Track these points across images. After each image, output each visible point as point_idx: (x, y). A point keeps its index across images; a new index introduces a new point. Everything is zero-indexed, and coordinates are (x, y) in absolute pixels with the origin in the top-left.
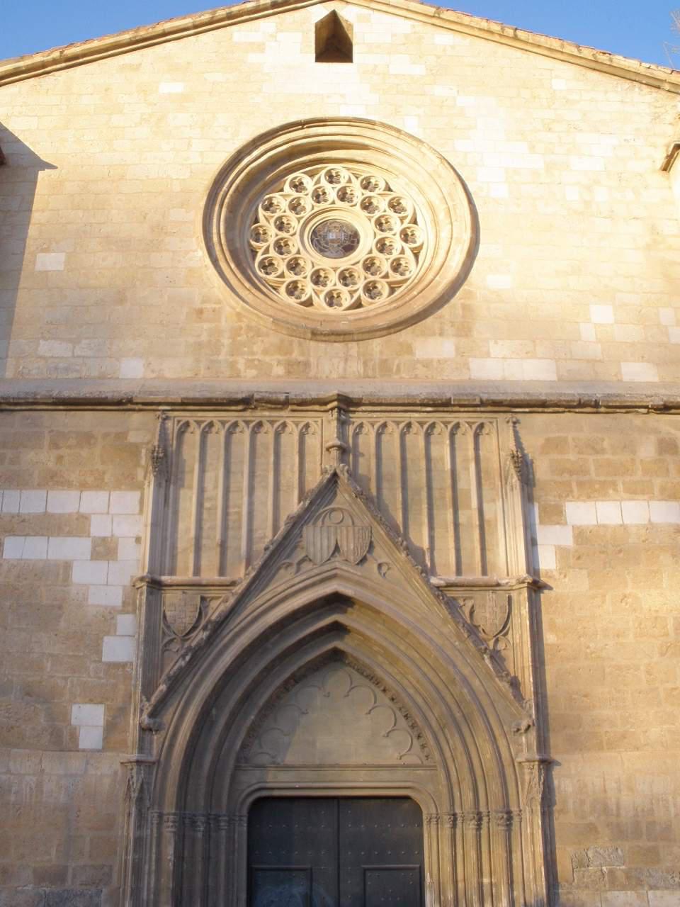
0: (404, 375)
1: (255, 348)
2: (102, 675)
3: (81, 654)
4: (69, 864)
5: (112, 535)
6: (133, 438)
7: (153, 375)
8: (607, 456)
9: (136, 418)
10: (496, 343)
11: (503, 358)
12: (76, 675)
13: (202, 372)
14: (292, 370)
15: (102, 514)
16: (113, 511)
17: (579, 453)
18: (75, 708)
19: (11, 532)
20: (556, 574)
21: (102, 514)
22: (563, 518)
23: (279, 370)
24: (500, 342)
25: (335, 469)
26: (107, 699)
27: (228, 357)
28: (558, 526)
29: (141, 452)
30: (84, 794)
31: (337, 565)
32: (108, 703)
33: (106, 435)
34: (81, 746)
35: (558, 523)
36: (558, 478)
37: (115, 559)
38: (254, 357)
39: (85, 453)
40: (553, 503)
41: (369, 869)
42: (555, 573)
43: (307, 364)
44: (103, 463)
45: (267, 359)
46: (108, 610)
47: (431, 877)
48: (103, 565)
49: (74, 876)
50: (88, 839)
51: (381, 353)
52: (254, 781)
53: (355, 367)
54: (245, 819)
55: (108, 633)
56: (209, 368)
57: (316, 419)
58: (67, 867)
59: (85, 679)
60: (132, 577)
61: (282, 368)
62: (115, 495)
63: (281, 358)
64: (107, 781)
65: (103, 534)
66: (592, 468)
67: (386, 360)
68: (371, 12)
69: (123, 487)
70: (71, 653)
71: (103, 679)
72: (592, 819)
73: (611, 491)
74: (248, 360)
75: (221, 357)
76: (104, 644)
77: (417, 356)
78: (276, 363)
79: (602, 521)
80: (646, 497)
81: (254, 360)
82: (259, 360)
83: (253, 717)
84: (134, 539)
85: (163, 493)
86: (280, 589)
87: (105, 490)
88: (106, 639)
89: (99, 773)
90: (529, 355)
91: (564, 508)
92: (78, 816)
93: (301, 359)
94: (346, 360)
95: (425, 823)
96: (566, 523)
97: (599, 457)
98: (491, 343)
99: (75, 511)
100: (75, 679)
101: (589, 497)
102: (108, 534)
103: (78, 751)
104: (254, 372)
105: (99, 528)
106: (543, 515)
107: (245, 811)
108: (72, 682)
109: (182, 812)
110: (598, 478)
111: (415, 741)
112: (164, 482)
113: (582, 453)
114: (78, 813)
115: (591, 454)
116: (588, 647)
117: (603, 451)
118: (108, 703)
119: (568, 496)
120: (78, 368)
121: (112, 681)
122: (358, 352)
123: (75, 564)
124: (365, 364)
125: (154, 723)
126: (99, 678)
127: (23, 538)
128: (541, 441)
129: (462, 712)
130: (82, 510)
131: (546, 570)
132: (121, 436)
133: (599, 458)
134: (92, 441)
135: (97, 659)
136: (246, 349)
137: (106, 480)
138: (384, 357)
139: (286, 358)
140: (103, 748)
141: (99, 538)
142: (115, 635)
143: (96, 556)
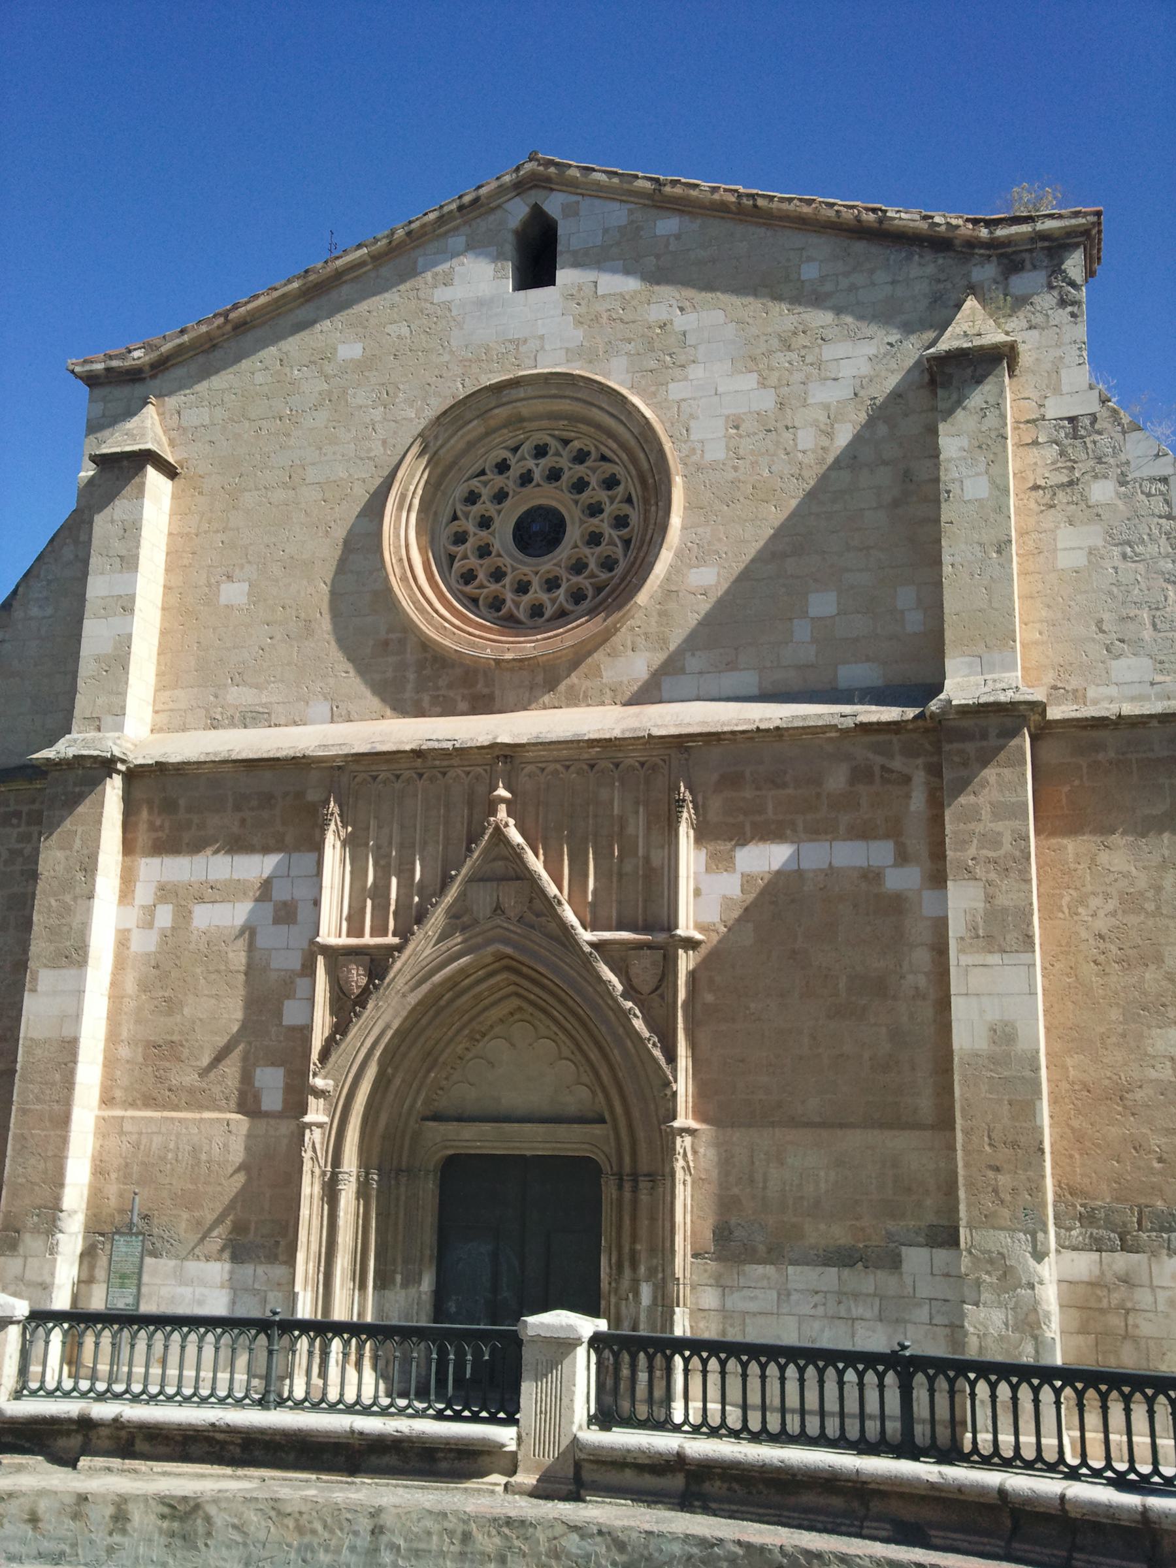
1: (441, 683)
8: (790, 791)
10: (693, 655)
11: (700, 673)
16: (292, 874)
18: (258, 1071)
19: (201, 899)
24: (698, 653)
34: (264, 1107)
45: (451, 694)
48: (284, 928)
50: (268, 1195)
55: (288, 998)
62: (295, 856)
63: (466, 692)
64: (285, 1141)
68: (580, 198)
73: (788, 832)
80: (829, 837)
81: (438, 696)
82: (444, 696)
83: (433, 1075)
88: (286, 1002)
93: (486, 691)
94: (531, 688)
98: (688, 655)
102: (289, 898)
116: (748, 1008)
117: (784, 785)
123: (259, 929)
127: (210, 905)
128: (715, 777)
132: (300, 795)
140: (285, 1109)
143: (277, 921)
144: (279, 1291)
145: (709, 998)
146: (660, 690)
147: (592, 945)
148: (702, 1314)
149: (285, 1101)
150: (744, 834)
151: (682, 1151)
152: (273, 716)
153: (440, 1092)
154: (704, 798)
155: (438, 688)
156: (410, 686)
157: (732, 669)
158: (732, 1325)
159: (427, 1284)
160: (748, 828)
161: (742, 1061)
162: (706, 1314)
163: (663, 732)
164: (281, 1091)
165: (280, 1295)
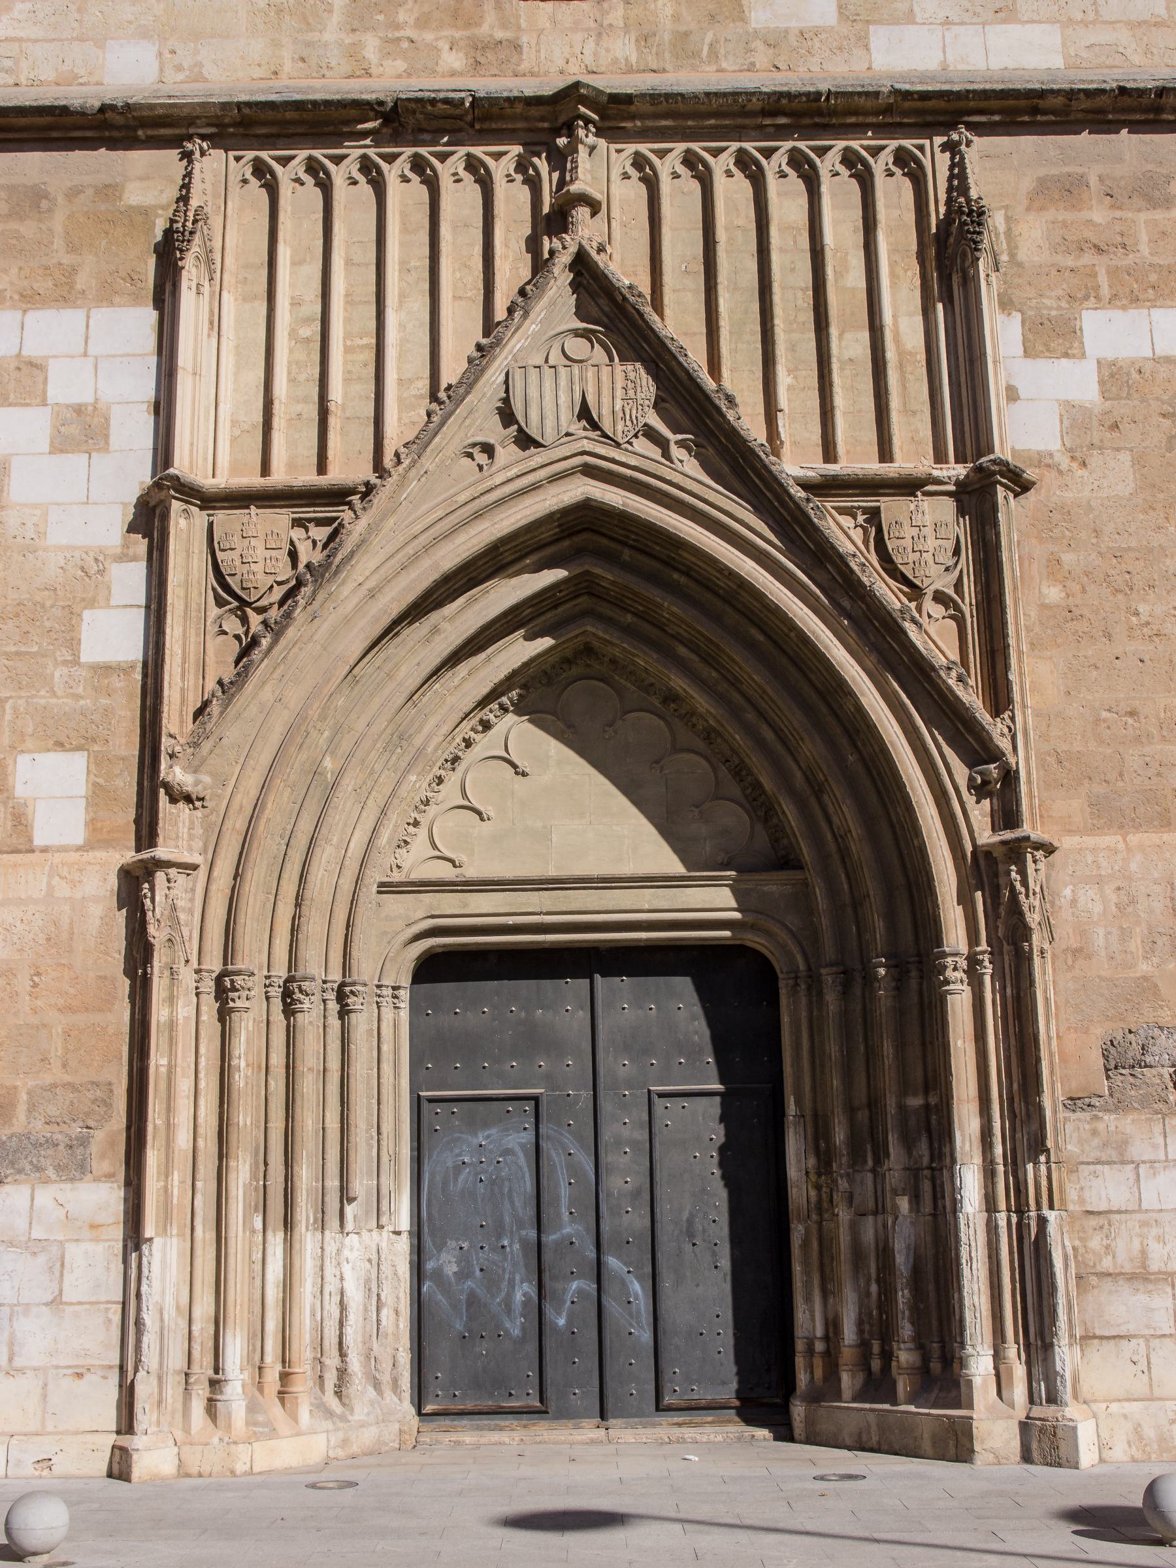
0: (724, 65)
1: (402, 16)
2: (80, 690)
3: (35, 649)
4: (18, 1083)
5: (96, 400)
6: (136, 195)
7: (180, 77)
9: (140, 159)
12: (23, 693)
13: (288, 67)
14: (482, 60)
15: (72, 357)
17: (1112, 207)
20: (1064, 462)
21: (72, 357)
22: (1076, 345)
23: (454, 60)
25: (580, 244)
26: (94, 740)
27: (343, 36)
28: (1064, 361)
29: (154, 224)
30: (48, 940)
31: (587, 446)
32: (96, 748)
33: (73, 193)
34: (38, 841)
35: (1066, 355)
36: (1070, 262)
37: (105, 448)
38: (397, 34)
39: (28, 229)
40: (1054, 313)
41: (662, 1095)
42: (1058, 457)
43: (517, 48)
44: (72, 248)
45: (429, 36)
46: (92, 554)
47: (798, 1103)
49: (32, 1109)
51: (676, 18)
52: (421, 914)
53: (624, 48)
54: (405, 994)
55: (91, 603)
56: (303, 60)
57: (537, 148)
58: (16, 1088)
59: (43, 701)
60: (142, 483)
61: (461, 55)
62: (102, 316)
63: (458, 34)
65: (76, 399)
66: (1144, 237)
67: (686, 34)
69: (117, 299)
70: (13, 649)
71: (82, 698)
72: (1144, 968)
74: (387, 41)
75: (329, 36)
76: (84, 627)
77: (754, 25)
78: (447, 47)
79: (1164, 348)
81: (399, 39)
84: (145, 406)
85: (207, 309)
86: (463, 498)
87: (75, 306)
88: (87, 614)
89: (79, 895)
90: (1000, 15)
91: (1078, 323)
92: (35, 985)
93: (500, 34)
95: (783, 992)
96: (1083, 355)
97: (1159, 215)
99: (15, 351)
100: (21, 702)
101: (1135, 300)
102: (88, 398)
103: (33, 851)
104: (400, 65)
106: (1030, 336)
107: (406, 980)
108: (15, 709)
109: (265, 973)
110: (1156, 260)
111: (759, 827)
112: (207, 284)
113: (1120, 208)
114: (36, 979)
115: (1139, 210)
116: (1137, 614)
118: (96, 748)
119: (1086, 298)
120: (8, 63)
121: (104, 701)
122: (626, 18)
123: (15, 463)
124: (645, 39)
125: (197, 783)
126: (77, 697)
128: (1027, 184)
129: (860, 753)
130: (29, 351)
131: (1038, 453)
132: (109, 191)
133: (1157, 217)
134: (44, 204)
135: (70, 658)
136: (381, 17)
137: (79, 287)
138: (683, 28)
139: (466, 33)
141: (67, 406)
142: (108, 607)
143: (61, 445)
144: (96, 1240)
145: (1053, 594)
146: (867, 47)
147: (806, 485)
148: (1093, 1222)
149: (92, 824)
150: (1097, 288)
151: (1038, 889)
152: (24, 64)
153: (411, 829)
154: (1008, 219)
155: (397, 27)
156: (336, 18)
157: (1004, 21)
158: (1161, 1239)
159: (404, 1221)
160: (1103, 279)
161: (1132, 714)
162: (1102, 1220)
163: (919, 88)
164: (83, 802)
165: (100, 1248)
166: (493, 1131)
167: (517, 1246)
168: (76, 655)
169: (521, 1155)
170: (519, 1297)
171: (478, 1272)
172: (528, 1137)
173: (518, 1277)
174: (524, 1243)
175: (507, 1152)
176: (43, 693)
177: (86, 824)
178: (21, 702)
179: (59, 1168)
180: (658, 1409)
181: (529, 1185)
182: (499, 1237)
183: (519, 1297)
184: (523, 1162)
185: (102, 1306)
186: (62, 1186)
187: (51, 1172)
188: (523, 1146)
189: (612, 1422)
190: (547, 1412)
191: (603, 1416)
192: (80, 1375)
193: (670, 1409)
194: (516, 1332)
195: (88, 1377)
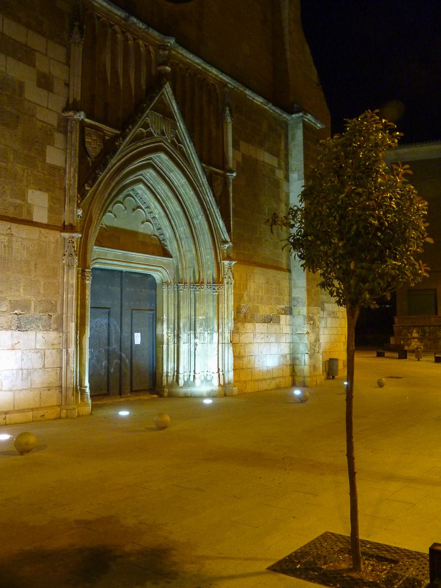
2: (46, 172)
18: (30, 191)
55: (49, 144)
88: (48, 146)
105: (42, 64)
126: (45, 175)
164: (47, 210)
166: (99, 319)
167: (103, 351)
168: (45, 160)
169: (105, 326)
170: (104, 363)
171: (95, 358)
172: (106, 321)
173: (103, 359)
174: (105, 350)
175: (102, 325)
176: (35, 170)
177: (48, 217)
178: (29, 171)
179: (44, 326)
180: (132, 391)
181: (106, 334)
182: (100, 348)
183: (104, 363)
184: (105, 328)
185: (55, 369)
186: (44, 332)
187: (41, 327)
188: (105, 324)
189: (123, 396)
190: (109, 394)
191: (120, 395)
192: (49, 390)
193: (137, 391)
194: (103, 374)
195: (51, 390)
